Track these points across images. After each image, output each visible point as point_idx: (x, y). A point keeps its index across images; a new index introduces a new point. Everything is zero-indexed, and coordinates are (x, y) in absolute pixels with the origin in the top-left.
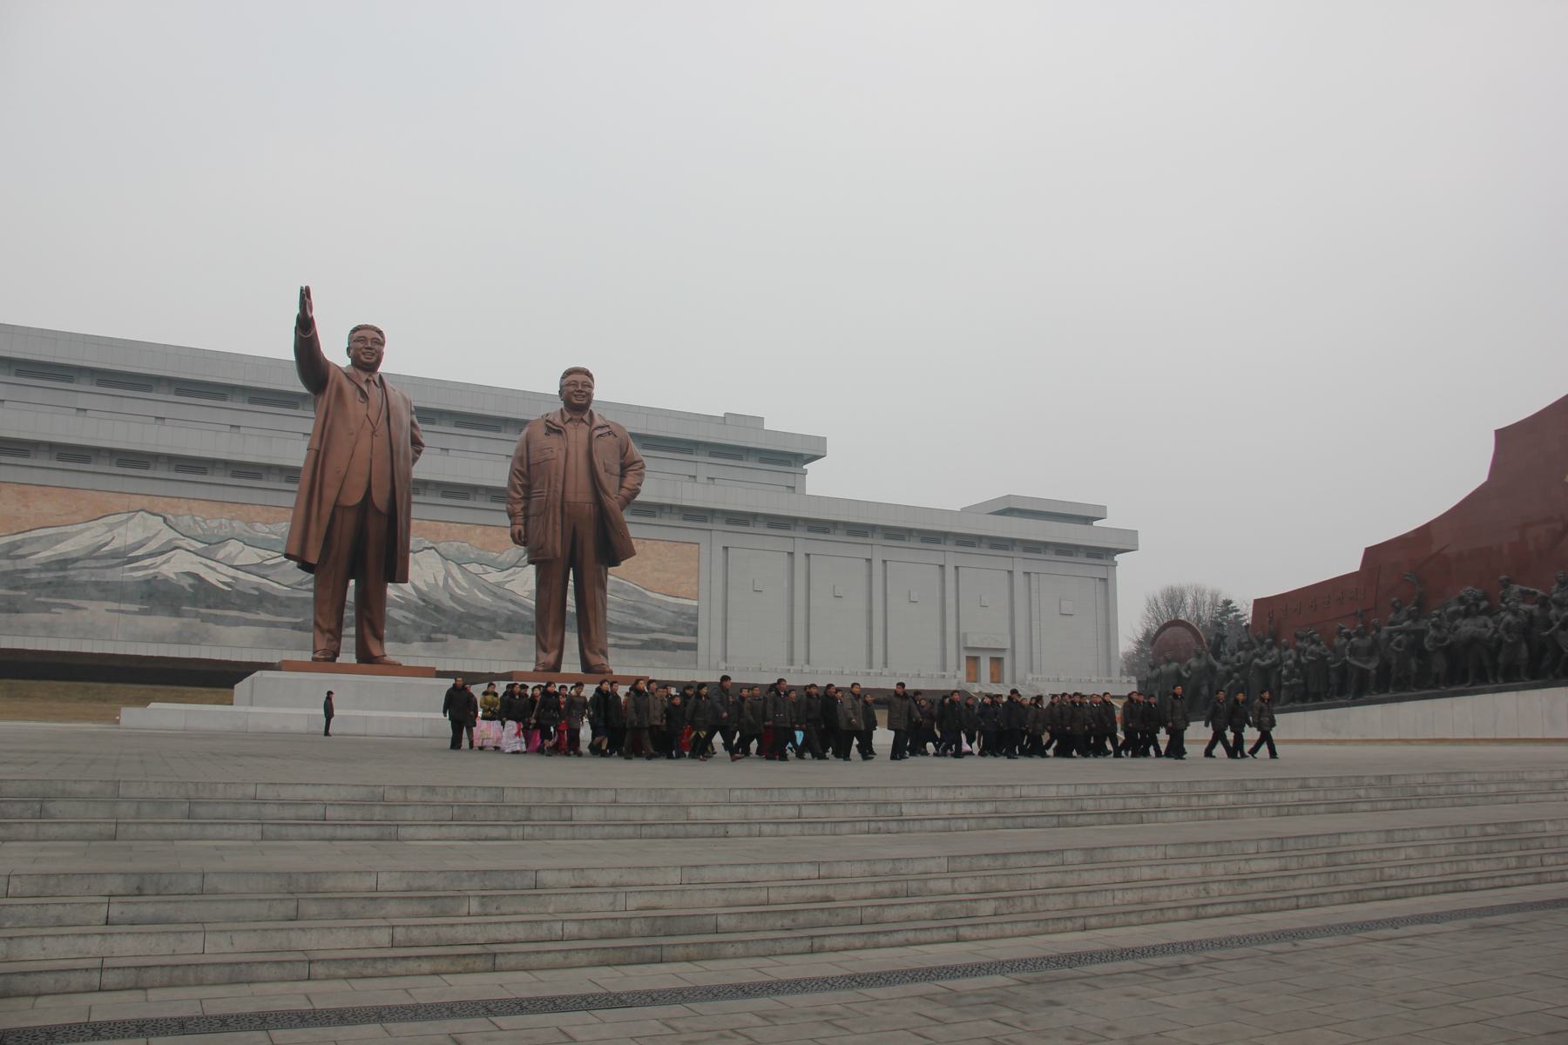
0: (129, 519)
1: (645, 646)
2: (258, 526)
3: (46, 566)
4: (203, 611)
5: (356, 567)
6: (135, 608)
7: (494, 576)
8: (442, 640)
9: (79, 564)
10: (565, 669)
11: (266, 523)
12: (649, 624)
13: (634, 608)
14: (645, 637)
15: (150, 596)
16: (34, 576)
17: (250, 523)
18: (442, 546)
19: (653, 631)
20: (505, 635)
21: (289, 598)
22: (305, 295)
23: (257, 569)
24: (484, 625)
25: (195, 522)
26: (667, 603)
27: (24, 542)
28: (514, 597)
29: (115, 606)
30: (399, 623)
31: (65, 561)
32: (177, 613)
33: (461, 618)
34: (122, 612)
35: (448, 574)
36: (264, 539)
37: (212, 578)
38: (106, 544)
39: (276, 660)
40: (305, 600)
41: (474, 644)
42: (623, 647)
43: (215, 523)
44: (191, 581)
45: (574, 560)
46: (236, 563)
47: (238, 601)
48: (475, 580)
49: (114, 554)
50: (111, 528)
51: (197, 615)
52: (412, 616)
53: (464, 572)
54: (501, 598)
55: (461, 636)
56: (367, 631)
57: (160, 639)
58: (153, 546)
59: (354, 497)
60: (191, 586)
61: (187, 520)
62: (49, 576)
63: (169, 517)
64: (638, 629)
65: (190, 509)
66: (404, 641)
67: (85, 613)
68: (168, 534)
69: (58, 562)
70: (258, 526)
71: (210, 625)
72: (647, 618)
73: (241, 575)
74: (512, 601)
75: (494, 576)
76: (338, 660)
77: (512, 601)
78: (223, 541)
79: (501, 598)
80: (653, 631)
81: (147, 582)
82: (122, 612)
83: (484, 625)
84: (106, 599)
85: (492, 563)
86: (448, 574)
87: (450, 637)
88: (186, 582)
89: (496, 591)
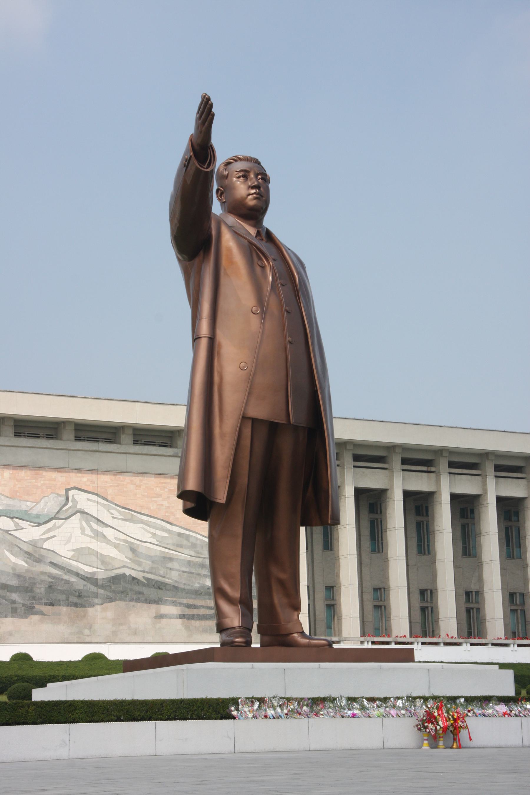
7: (29, 533)
22: (206, 113)
42: (192, 617)
54: (39, 560)
74: (52, 564)
75: (29, 533)
77: (52, 564)
79: (39, 560)
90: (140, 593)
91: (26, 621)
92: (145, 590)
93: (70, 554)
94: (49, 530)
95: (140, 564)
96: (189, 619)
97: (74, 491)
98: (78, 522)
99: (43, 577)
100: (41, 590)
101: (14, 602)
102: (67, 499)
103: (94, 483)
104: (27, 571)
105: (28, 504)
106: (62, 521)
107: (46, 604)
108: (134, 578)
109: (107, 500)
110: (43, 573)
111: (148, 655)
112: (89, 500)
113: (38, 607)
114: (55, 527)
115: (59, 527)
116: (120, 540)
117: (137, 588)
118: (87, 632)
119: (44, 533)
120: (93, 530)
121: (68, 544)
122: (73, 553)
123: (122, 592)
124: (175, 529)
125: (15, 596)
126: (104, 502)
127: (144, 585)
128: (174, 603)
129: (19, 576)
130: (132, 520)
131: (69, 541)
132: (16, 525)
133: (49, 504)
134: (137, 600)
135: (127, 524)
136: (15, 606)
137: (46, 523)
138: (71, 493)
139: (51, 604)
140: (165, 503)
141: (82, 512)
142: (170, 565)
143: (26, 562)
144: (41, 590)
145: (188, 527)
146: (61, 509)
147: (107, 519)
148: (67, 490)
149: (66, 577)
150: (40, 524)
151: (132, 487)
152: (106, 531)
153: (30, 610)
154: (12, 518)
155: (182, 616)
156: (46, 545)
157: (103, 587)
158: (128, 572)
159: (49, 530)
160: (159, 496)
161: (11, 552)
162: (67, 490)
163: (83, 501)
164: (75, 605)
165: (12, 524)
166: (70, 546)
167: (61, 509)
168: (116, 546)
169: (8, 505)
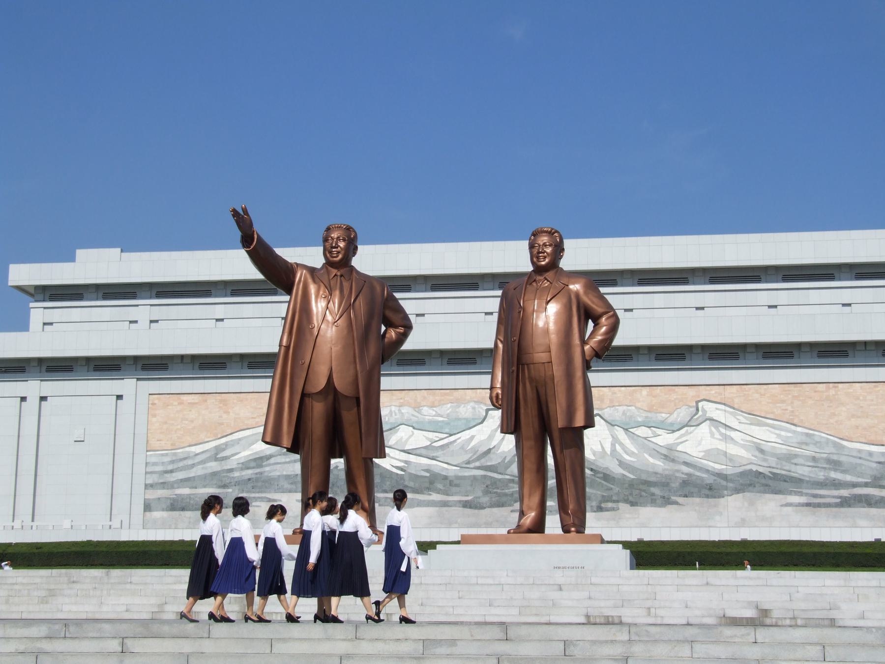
1: (845, 502)
2: (425, 410)
3: (245, 466)
7: (664, 439)
8: (613, 509)
9: (272, 461)
10: (548, 531)
11: (432, 406)
12: (849, 478)
13: (829, 461)
14: (845, 493)
16: (236, 474)
17: (417, 407)
19: (854, 485)
20: (680, 500)
21: (458, 478)
23: (427, 452)
24: (656, 491)
26: (871, 454)
27: (226, 445)
31: (261, 458)
33: (632, 485)
35: (615, 440)
36: (430, 422)
40: (474, 478)
41: (646, 512)
42: (819, 505)
45: (544, 427)
46: (407, 448)
48: (644, 444)
53: (633, 437)
54: (673, 461)
55: (633, 504)
59: (321, 383)
62: (249, 473)
64: (837, 484)
69: (255, 460)
70: (425, 410)
72: (844, 472)
73: (412, 458)
74: (686, 464)
75: (664, 439)
77: (686, 464)
80: (854, 485)
83: (656, 491)
85: (661, 425)
87: (623, 506)
90: (767, 485)
91: (663, 510)
92: (770, 482)
93: (701, 455)
95: (765, 460)
96: (814, 507)
97: (704, 403)
98: (707, 427)
99: (677, 475)
100: (675, 485)
101: (653, 494)
102: (697, 410)
103: (721, 394)
104: (664, 470)
105: (663, 415)
106: (693, 428)
107: (680, 496)
108: (760, 473)
109: (734, 408)
110: (678, 471)
111: (738, 539)
112: (717, 409)
113: (673, 498)
114: (687, 433)
116: (747, 441)
117: (763, 481)
118: (717, 518)
119: (678, 438)
120: (721, 434)
121: (699, 445)
122: (703, 454)
123: (750, 485)
124: (799, 429)
125: (653, 490)
126: (732, 410)
127: (770, 478)
128: (801, 494)
129: (656, 473)
130: (759, 424)
131: (700, 444)
134: (765, 492)
135: (753, 427)
137: (678, 430)
138: (700, 404)
139: (686, 496)
140: (790, 408)
141: (711, 420)
142: (795, 461)
144: (675, 485)
145: (812, 427)
147: (733, 423)
148: (697, 402)
149: (698, 474)
150: (674, 431)
151: (757, 396)
152: (733, 434)
153: (667, 501)
155: (808, 505)
156: (680, 448)
157: (732, 481)
158: (754, 468)
160: (783, 402)
161: (650, 455)
162: (697, 402)
163: (711, 410)
164: (707, 496)
165: (650, 432)
166: (701, 448)
168: (743, 446)
169: (646, 417)
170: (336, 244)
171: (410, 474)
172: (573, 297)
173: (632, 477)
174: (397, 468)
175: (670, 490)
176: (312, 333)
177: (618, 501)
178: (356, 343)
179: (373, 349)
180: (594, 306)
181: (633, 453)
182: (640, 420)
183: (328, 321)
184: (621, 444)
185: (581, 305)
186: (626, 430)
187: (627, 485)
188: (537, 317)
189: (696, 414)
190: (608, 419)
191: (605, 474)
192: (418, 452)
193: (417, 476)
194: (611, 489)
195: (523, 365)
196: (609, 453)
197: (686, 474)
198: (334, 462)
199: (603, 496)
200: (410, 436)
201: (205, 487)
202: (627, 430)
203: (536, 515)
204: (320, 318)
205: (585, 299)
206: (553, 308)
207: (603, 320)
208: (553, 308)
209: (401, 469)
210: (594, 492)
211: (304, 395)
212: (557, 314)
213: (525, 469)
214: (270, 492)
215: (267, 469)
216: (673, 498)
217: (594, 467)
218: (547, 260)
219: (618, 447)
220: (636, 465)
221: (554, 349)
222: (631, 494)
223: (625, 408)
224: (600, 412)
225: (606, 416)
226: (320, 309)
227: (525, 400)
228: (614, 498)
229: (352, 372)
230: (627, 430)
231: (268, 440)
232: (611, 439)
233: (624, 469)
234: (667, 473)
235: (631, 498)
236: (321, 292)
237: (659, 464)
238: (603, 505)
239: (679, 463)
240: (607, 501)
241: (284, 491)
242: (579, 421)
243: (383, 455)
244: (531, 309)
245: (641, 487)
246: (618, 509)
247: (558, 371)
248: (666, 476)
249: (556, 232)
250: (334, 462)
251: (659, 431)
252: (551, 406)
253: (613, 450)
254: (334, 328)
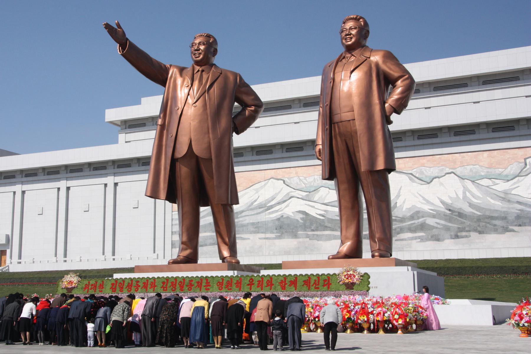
0: (265, 185)
4: (310, 233)
5: (202, 197)
6: (273, 236)
7: (501, 186)
8: (466, 237)
9: (244, 214)
15: (281, 227)
18: (458, 171)
20: (516, 228)
25: (300, 180)
28: (520, 200)
29: (263, 235)
30: (434, 227)
32: (296, 236)
33: (479, 219)
34: (267, 238)
35: (465, 189)
37: (313, 212)
38: (255, 201)
39: (279, 262)
41: (491, 238)
43: (311, 179)
44: (301, 216)
46: (325, 202)
47: (329, 225)
49: (260, 206)
50: (257, 191)
51: (308, 236)
52: (443, 222)
54: (509, 201)
55: (480, 233)
56: (220, 240)
57: (288, 253)
58: (279, 198)
59: (182, 150)
60: (302, 219)
61: (296, 179)
63: (286, 179)
65: (297, 173)
66: (438, 240)
67: (248, 241)
68: (287, 190)
71: (315, 242)
73: (329, 208)
74: (519, 203)
75: (501, 186)
76: (199, 263)
77: (519, 203)
78: (316, 190)
81: (278, 219)
82: (267, 238)
84: (258, 233)
85: (499, 177)
86: (465, 189)
87: (473, 234)
88: (299, 217)
89: (505, 197)
94: (515, 183)
100: (511, 218)
101: (495, 225)
102: (526, 164)
104: (502, 208)
105: (500, 170)
107: (516, 226)
110: (513, 208)
113: (511, 227)
114: (518, 181)
115: (522, 181)
132: (493, 182)
133: (514, 168)
136: (495, 227)
137: (512, 179)
138: (528, 161)
139: (520, 225)
143: (501, 203)
144: (511, 218)
146: (522, 170)
148: (525, 159)
150: (508, 181)
153: (506, 230)
154: (490, 179)
156: (513, 192)
159: (515, 183)
161: (492, 198)
162: (525, 159)
167: (522, 170)
169: (488, 172)
170: (198, 47)
171: (328, 218)
172: (373, 66)
173: (479, 214)
174: (320, 215)
175: (507, 222)
176: (177, 113)
177: (470, 231)
178: (209, 118)
179: (224, 122)
180: (391, 72)
181: (479, 197)
182: (483, 174)
183: (189, 104)
184: (470, 192)
185: (381, 73)
186: (473, 182)
187: (475, 220)
188: (343, 84)
189: (524, 168)
190: (460, 175)
191: (459, 213)
192: (333, 204)
193: (332, 219)
194: (464, 223)
195: (334, 123)
196: (461, 198)
197: (520, 210)
198: (202, 209)
199: (459, 228)
200: (327, 194)
201: (205, 232)
202: (474, 181)
203: (352, 244)
204: (183, 102)
205: (383, 67)
206: (356, 76)
207: (399, 83)
208: (356, 76)
209: (323, 216)
210: (453, 225)
211: (174, 161)
212: (359, 80)
213: (342, 208)
214: (243, 234)
215: (241, 219)
216: (511, 227)
217: (451, 208)
218: (353, 40)
219: (468, 194)
220: (482, 206)
221: (356, 108)
222: (479, 226)
223: (472, 166)
224: (454, 171)
225: (458, 173)
226: (183, 95)
227: (338, 152)
228: (467, 229)
229: (206, 140)
230: (474, 181)
231: (148, 195)
232: (462, 189)
233: (472, 208)
234: (505, 210)
235: (479, 229)
236: (185, 83)
237: (498, 205)
238: (459, 234)
239: (513, 202)
240: (462, 231)
241: (251, 233)
242: (380, 165)
243: (237, 203)
244: (339, 79)
245: (486, 220)
246: (470, 236)
247: (359, 126)
248: (504, 212)
249: (361, 18)
250: (202, 209)
251: (497, 181)
252: (357, 154)
253: (465, 197)
254: (193, 108)
